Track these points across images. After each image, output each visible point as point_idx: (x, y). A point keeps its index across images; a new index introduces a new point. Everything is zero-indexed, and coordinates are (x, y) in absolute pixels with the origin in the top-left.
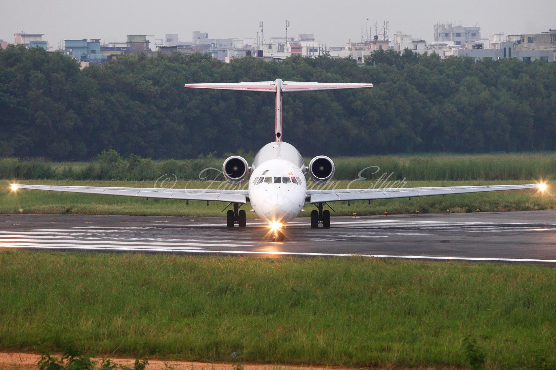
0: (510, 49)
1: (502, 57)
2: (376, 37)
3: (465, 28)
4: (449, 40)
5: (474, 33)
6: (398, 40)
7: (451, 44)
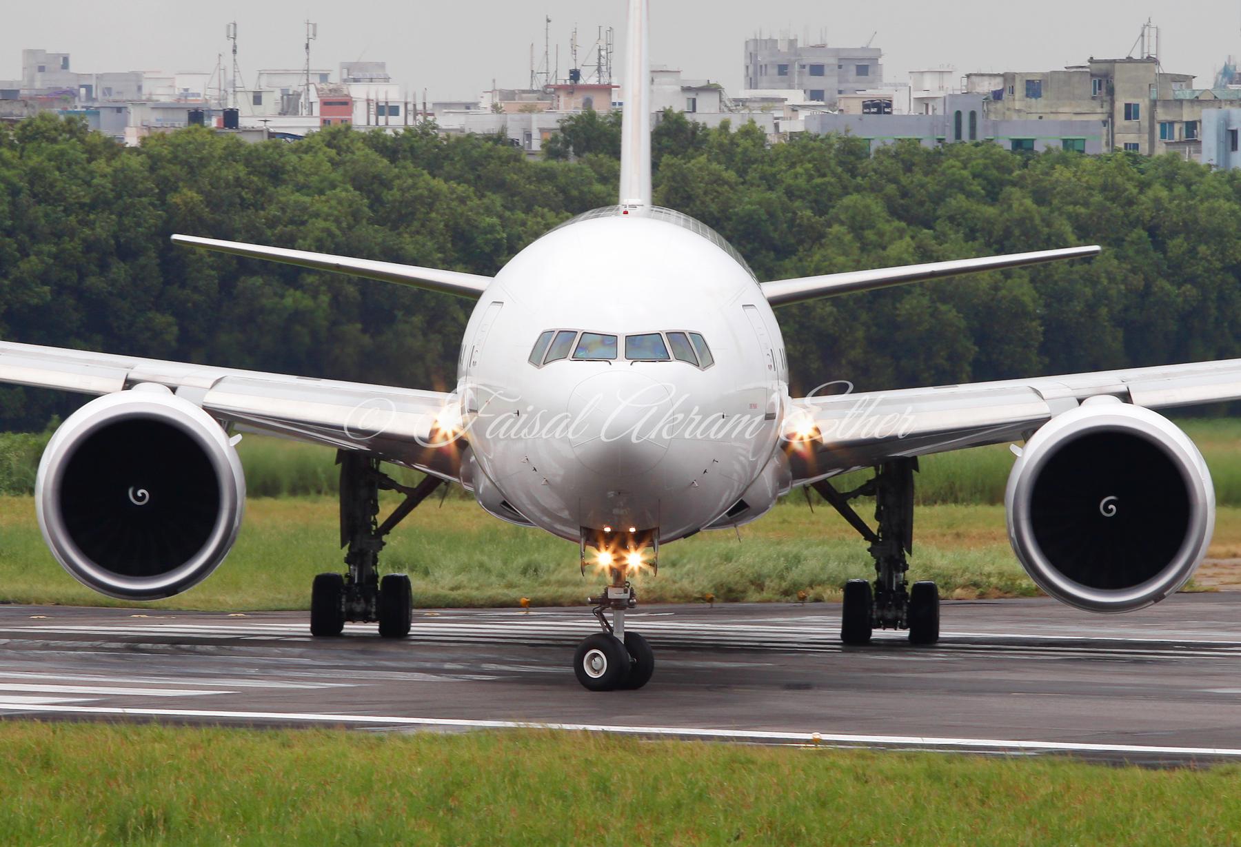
0: (973, 115)
1: (950, 138)
4: (791, 87)
5: (865, 67)
7: (796, 97)
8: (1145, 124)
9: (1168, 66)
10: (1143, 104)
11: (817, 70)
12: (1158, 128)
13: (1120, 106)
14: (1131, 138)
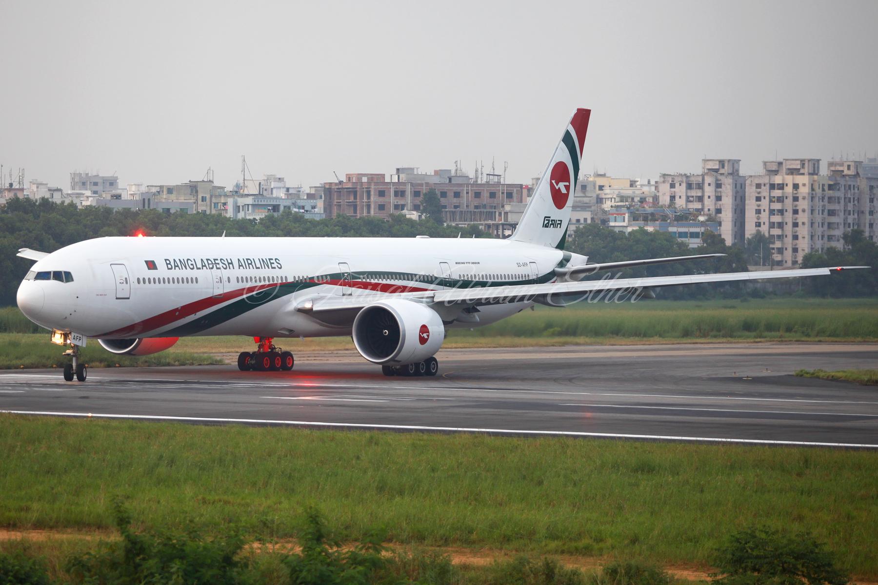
0: (149, 200)
1: (141, 208)
2: (11, 185)
3: (103, 177)
4: (87, 190)
5: (112, 182)
6: (34, 188)
7: (88, 193)
8: (209, 203)
9: (217, 183)
10: (208, 197)
11: (96, 184)
12: (213, 204)
13: (200, 197)
14: (204, 208)
